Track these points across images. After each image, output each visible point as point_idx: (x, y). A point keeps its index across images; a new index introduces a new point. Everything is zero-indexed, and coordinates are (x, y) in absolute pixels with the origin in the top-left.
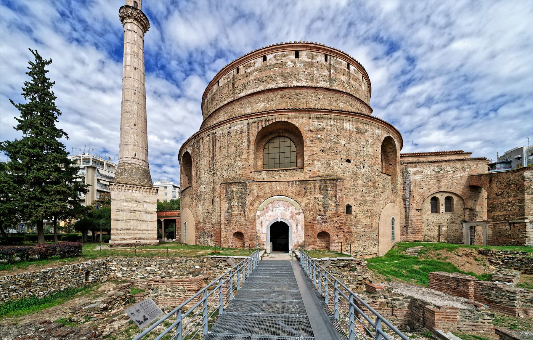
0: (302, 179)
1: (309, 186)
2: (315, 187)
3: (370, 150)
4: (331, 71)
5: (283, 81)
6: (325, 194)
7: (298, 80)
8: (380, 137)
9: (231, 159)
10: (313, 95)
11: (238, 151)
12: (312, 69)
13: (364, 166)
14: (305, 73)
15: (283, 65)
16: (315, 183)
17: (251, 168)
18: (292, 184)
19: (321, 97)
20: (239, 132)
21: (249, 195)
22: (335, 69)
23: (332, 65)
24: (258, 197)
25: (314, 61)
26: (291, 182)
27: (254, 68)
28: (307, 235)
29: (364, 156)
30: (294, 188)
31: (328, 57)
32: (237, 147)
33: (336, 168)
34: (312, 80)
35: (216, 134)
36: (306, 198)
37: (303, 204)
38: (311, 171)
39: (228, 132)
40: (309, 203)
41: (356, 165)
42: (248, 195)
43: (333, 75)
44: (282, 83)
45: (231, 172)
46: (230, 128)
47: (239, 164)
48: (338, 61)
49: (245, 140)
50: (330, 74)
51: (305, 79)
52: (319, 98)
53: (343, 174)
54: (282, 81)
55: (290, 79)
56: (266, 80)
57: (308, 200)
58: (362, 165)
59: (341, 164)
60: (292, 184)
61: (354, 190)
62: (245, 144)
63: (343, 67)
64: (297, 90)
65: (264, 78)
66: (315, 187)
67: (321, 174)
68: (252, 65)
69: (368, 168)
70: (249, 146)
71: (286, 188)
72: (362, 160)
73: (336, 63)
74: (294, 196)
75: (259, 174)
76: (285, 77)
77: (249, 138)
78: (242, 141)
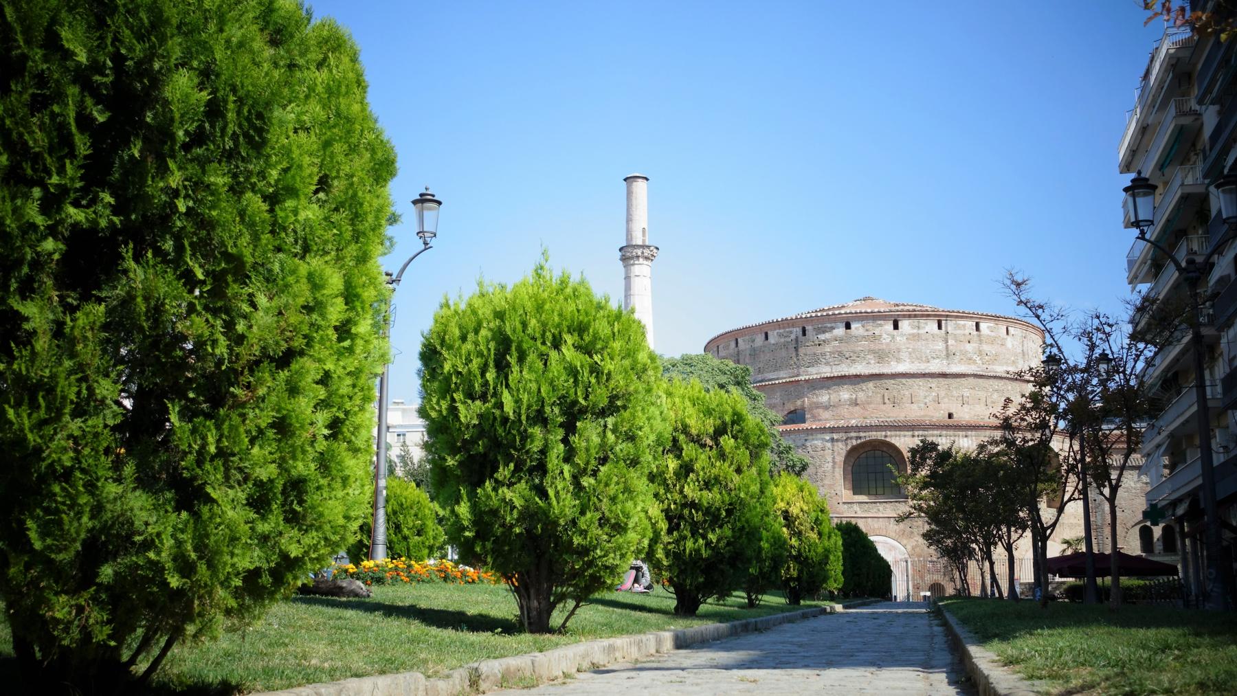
4: (947, 342)
7: (898, 360)
12: (919, 343)
15: (875, 338)
19: (933, 385)
22: (955, 337)
25: (921, 331)
31: (943, 322)
34: (919, 359)
37: (909, 547)
40: (917, 546)
43: (951, 348)
49: (830, 459)
50: (947, 346)
63: (967, 332)
70: (834, 467)
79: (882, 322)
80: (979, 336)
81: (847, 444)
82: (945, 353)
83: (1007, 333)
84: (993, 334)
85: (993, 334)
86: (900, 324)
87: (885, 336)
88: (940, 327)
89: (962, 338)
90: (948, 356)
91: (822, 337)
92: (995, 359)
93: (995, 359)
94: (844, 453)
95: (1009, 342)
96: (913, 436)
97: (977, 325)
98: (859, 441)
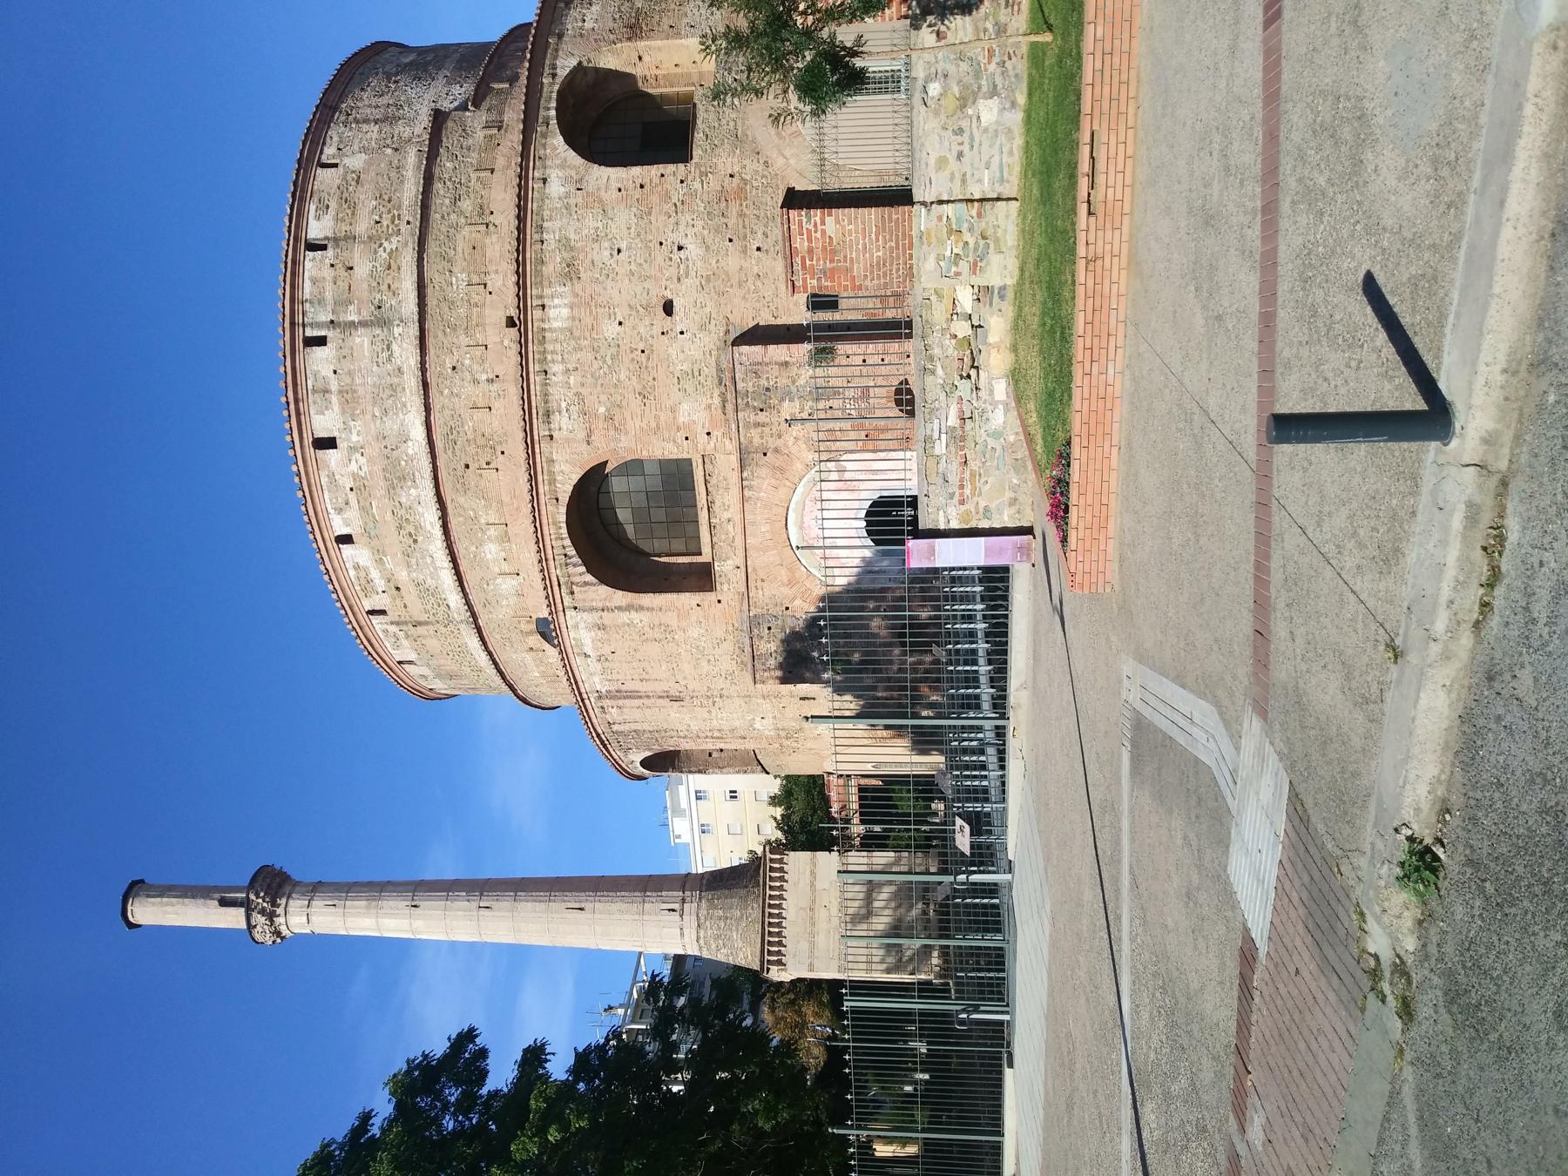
0: (734, 459)
1: (757, 441)
2: (757, 425)
3: (624, 218)
4: (352, 325)
5: (409, 483)
6: (779, 395)
8: (573, 173)
9: (680, 654)
10: (446, 391)
11: (658, 636)
13: (680, 248)
14: (377, 414)
16: (747, 426)
17: (706, 604)
18: (750, 488)
19: (449, 365)
20: (600, 633)
21: (787, 608)
22: (342, 303)
23: (330, 317)
24: (791, 583)
26: (746, 492)
27: (372, 569)
28: (906, 442)
29: (646, 246)
30: (762, 480)
32: (645, 637)
33: (695, 352)
35: (603, 691)
36: (794, 449)
38: (708, 434)
39: (599, 661)
41: (679, 279)
42: (788, 612)
43: (366, 315)
44: (416, 487)
45: (718, 652)
46: (586, 655)
47: (694, 632)
48: (311, 293)
49: (624, 617)
50: (363, 324)
51: (397, 414)
52: (454, 368)
53: (712, 327)
54: (410, 488)
55: (403, 463)
56: (410, 534)
57: (800, 443)
58: (676, 256)
59: (682, 333)
60: (750, 488)
61: (759, 283)
62: (633, 615)
63: (328, 273)
64: (439, 444)
65: (405, 540)
66: (757, 425)
67: (717, 401)
68: (362, 574)
69: (682, 228)
70: (641, 608)
71: (765, 507)
72: (660, 255)
73: (319, 303)
74: (788, 483)
75: (723, 579)
76: (397, 477)
77: (619, 608)
78: (628, 625)
79: (323, 474)
80: (336, 240)
81: (586, 584)
82: (378, 331)
83: (335, 165)
84: (333, 205)
85: (333, 205)
86: (321, 435)
87: (353, 467)
88: (321, 341)
89: (343, 285)
90: (384, 323)
91: (380, 584)
92: (386, 199)
93: (386, 199)
94: (604, 590)
95: (355, 161)
96: (551, 437)
97: (313, 247)
98: (577, 560)
